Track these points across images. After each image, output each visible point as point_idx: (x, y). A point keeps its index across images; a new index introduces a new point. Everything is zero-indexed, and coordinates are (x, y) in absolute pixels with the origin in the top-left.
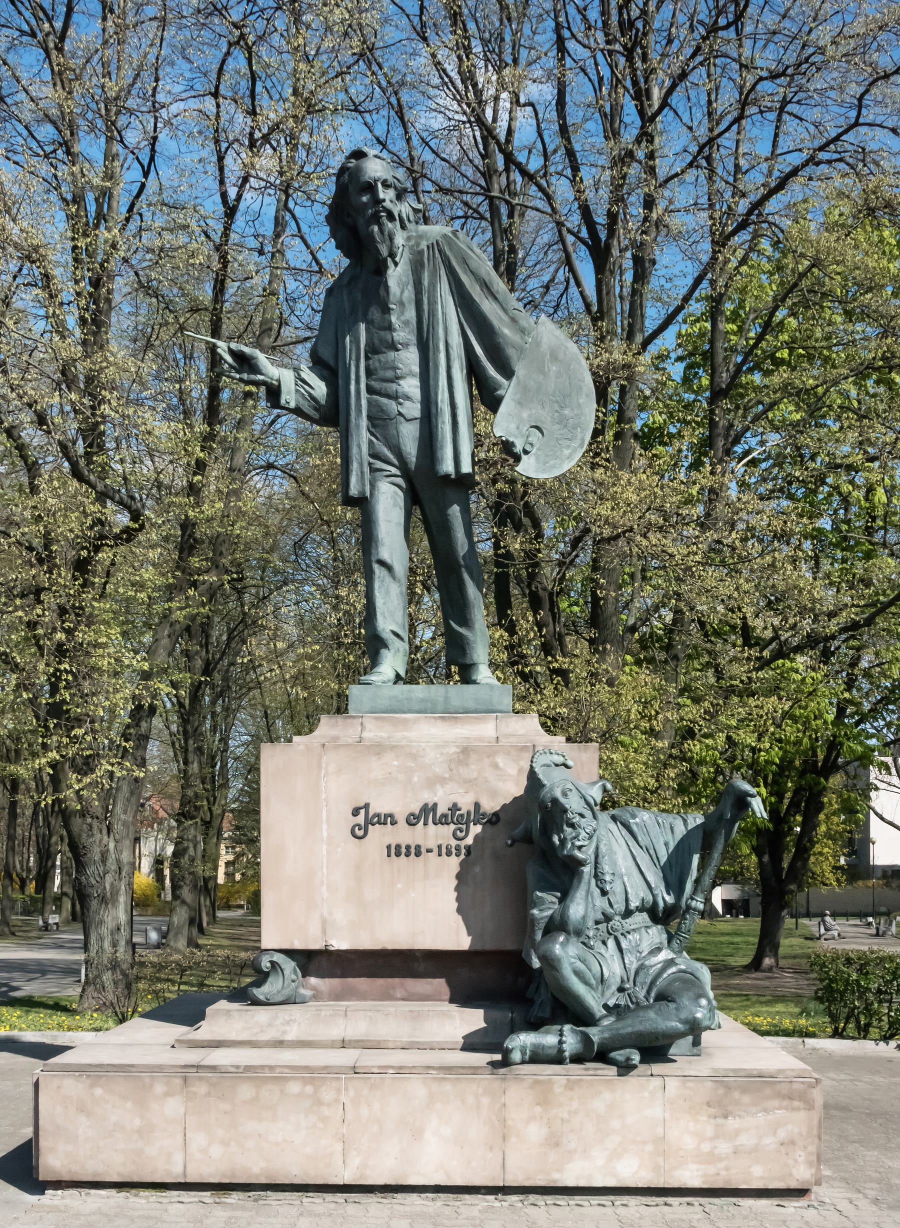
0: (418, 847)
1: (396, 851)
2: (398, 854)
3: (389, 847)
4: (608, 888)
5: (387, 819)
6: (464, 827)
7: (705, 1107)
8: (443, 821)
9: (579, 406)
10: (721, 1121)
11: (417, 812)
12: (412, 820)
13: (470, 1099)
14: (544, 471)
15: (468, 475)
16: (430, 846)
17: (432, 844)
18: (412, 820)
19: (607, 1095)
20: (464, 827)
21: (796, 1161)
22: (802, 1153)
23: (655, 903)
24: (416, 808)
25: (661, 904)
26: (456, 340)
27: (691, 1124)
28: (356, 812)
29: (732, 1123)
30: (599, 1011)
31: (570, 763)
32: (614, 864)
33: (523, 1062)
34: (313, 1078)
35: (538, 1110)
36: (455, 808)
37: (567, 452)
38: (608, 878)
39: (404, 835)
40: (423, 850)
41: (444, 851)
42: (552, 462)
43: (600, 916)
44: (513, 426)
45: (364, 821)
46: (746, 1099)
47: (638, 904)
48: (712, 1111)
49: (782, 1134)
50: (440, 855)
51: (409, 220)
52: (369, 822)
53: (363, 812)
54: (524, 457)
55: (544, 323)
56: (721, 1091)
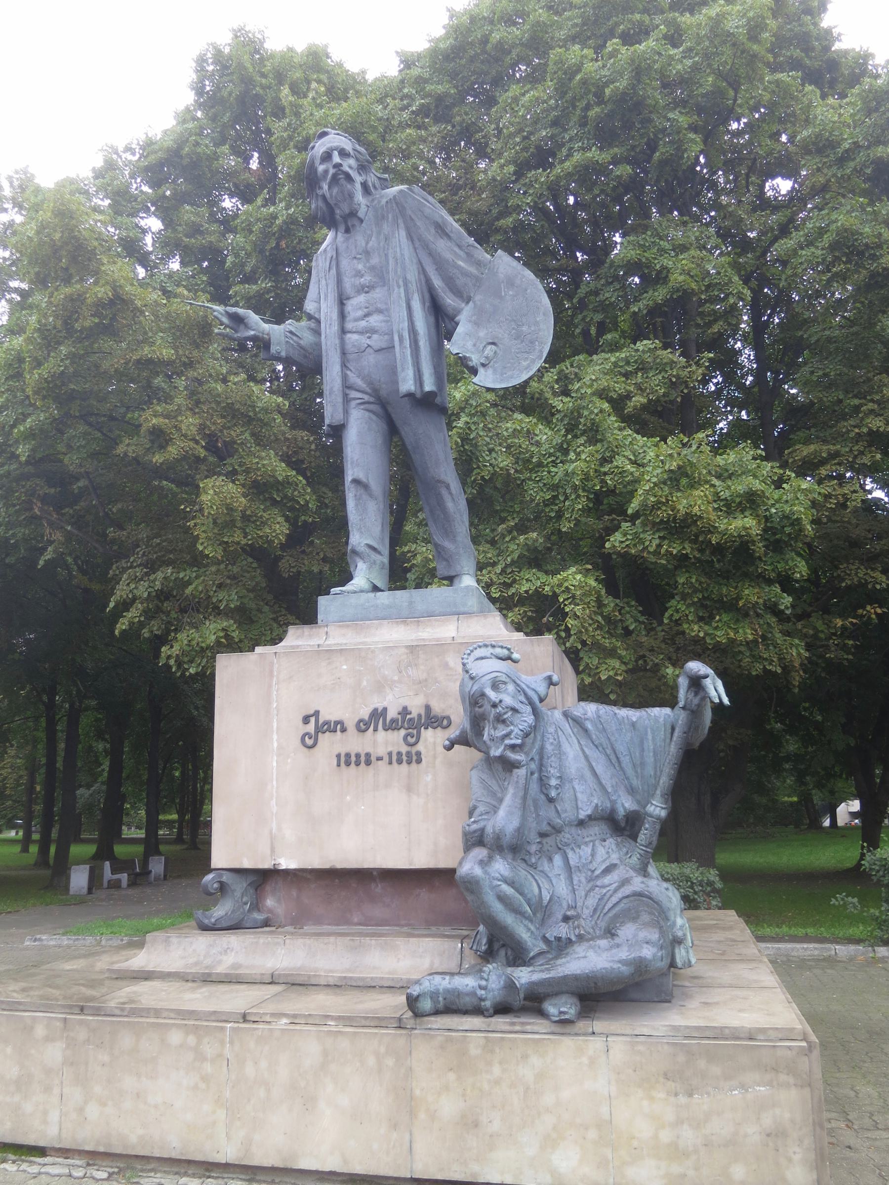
0: (368, 755)
1: (346, 760)
2: (348, 764)
3: (338, 756)
4: (553, 794)
5: (336, 727)
6: (415, 732)
7: (662, 1080)
8: (393, 726)
9: (537, 323)
10: (683, 1099)
11: (366, 718)
12: (363, 726)
13: (371, 1061)
14: (502, 381)
15: (430, 393)
16: (380, 754)
17: (381, 751)
18: (363, 726)
19: (535, 1061)
20: (415, 732)
21: (790, 1160)
22: (797, 1149)
23: (613, 811)
24: (365, 713)
25: (621, 812)
26: (413, 275)
27: (645, 1103)
28: (306, 720)
29: (701, 1103)
30: (535, 946)
31: (515, 656)
32: (561, 768)
33: (437, 1013)
34: (197, 1027)
35: (452, 1076)
36: (405, 711)
37: (525, 364)
38: (553, 782)
39: (354, 743)
40: (373, 759)
41: (394, 758)
42: (509, 373)
43: (545, 828)
44: (469, 344)
45: (317, 728)
46: (716, 1070)
47: (589, 812)
48: (671, 1085)
49: (767, 1120)
50: (390, 763)
51: (375, 188)
52: (319, 730)
53: (313, 719)
54: (481, 371)
55: (500, 257)
56: (681, 1058)
